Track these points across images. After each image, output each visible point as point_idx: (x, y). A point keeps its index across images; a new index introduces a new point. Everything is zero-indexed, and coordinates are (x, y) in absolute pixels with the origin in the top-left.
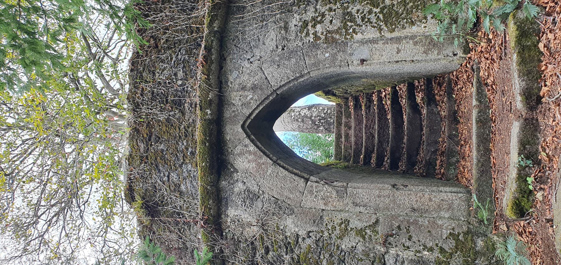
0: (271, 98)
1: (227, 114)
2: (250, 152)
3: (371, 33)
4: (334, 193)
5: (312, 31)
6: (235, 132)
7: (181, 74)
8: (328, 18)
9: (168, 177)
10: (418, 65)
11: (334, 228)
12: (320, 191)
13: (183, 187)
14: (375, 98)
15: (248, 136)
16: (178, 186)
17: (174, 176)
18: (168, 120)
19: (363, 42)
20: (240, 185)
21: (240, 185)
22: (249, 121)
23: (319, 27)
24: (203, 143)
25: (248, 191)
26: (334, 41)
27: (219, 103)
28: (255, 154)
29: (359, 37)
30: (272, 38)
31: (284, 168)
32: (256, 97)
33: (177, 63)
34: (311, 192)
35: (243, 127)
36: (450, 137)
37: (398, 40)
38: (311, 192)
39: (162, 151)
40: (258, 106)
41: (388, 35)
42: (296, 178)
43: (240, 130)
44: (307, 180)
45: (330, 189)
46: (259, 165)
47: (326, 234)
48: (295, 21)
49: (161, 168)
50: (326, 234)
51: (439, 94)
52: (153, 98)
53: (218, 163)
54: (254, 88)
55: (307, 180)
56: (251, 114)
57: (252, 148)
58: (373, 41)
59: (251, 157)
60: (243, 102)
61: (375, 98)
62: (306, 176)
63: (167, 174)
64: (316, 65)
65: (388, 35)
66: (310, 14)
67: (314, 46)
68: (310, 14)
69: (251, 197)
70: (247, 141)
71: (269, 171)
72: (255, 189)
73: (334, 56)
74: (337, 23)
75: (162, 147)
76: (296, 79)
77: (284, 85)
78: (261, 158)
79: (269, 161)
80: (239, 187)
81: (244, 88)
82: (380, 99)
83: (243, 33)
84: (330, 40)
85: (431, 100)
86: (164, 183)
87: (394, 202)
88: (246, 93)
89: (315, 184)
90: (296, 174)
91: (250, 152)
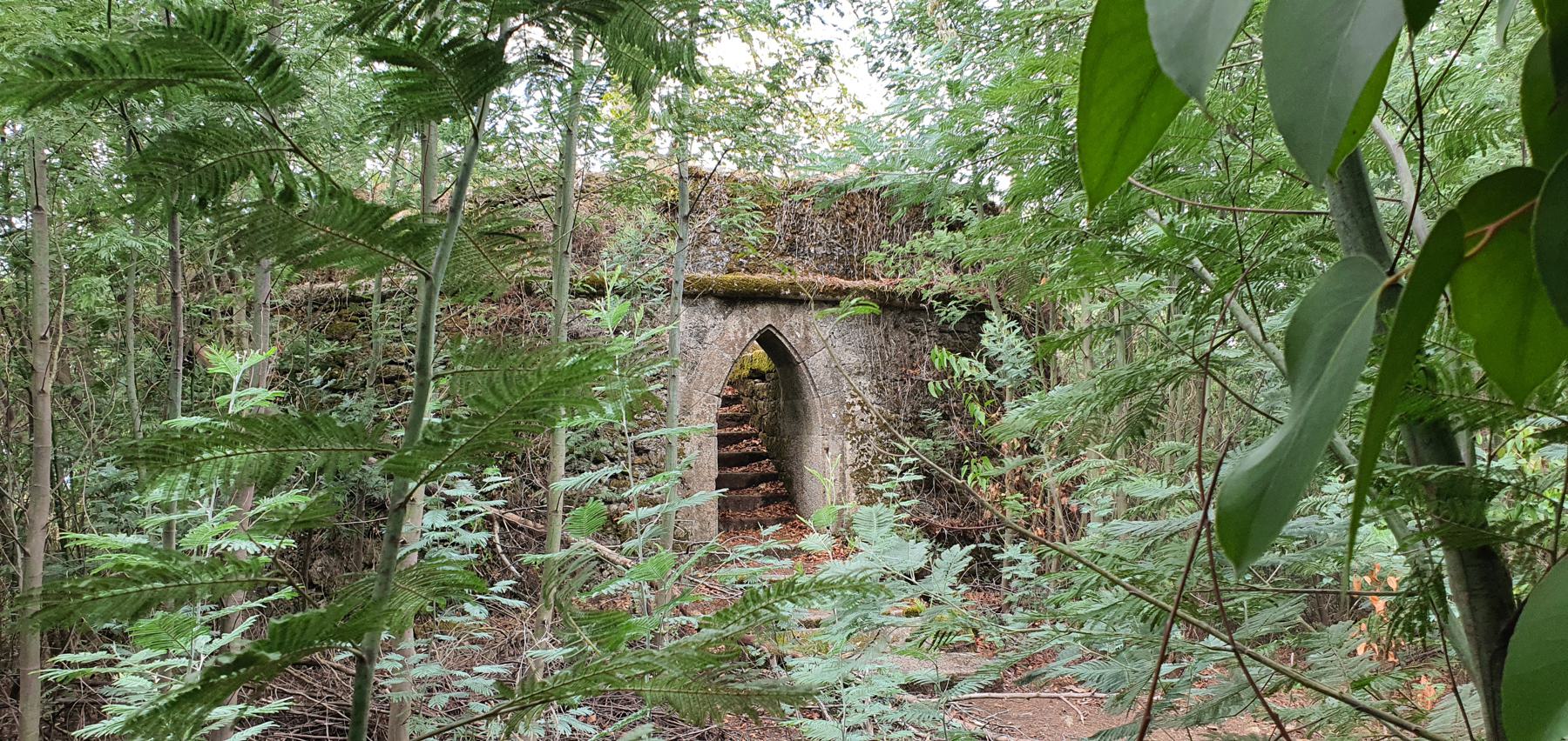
1: (782, 308)
3: (850, 457)
5: (855, 400)
6: (764, 316)
7: (821, 251)
8: (866, 417)
10: (819, 497)
13: (703, 250)
14: (746, 429)
16: (705, 243)
17: (715, 239)
19: (843, 449)
20: (711, 322)
21: (711, 322)
23: (858, 408)
26: (846, 423)
27: (795, 301)
28: (744, 339)
29: (848, 445)
30: (851, 358)
33: (831, 247)
34: (708, 401)
36: (742, 522)
37: (843, 480)
38: (708, 401)
41: (848, 472)
46: (732, 345)
48: (864, 381)
51: (777, 509)
52: (799, 217)
53: (733, 299)
54: (807, 339)
58: (843, 459)
60: (793, 327)
61: (746, 429)
64: (826, 405)
65: (848, 472)
66: (870, 399)
67: (843, 402)
68: (870, 399)
69: (700, 337)
70: (755, 331)
72: (709, 340)
73: (832, 422)
74: (861, 426)
81: (807, 328)
82: (748, 437)
83: (857, 326)
84: (847, 418)
85: (768, 500)
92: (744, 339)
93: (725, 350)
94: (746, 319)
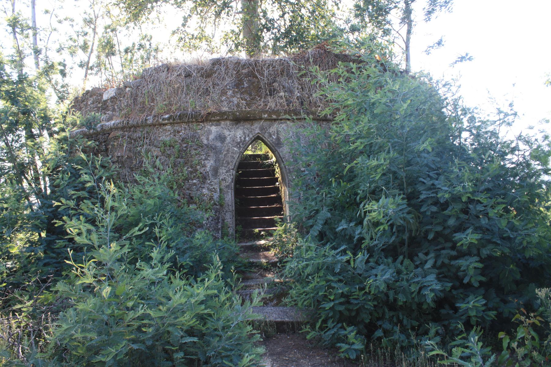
2: (245, 138)
4: (228, 184)
11: (212, 185)
22: (261, 136)
39: (243, 84)
42: (234, 164)
43: (257, 132)
44: (233, 169)
45: (229, 181)
46: (239, 143)
47: (209, 182)
50: (209, 182)
55: (233, 169)
59: (242, 138)
62: (235, 169)
70: (251, 136)
75: (246, 85)
76: (283, 162)
77: (280, 155)
78: (243, 144)
86: (226, 86)
87: (226, 212)
88: (276, 135)
89: (231, 174)
91: (245, 138)
92: (245, 141)
93: (235, 147)
94: (247, 132)
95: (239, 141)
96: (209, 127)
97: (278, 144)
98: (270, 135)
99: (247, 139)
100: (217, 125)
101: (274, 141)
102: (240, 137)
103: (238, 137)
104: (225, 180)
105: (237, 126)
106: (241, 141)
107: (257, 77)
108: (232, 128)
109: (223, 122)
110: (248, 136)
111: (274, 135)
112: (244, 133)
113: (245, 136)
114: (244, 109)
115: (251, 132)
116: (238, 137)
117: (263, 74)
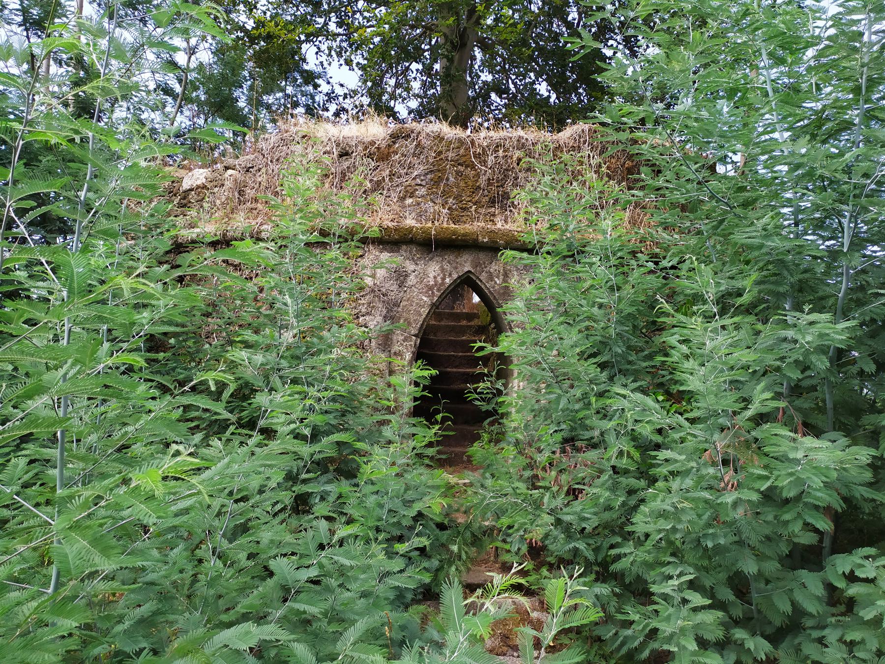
0: (495, 302)
1: (482, 256)
2: (443, 279)
6: (466, 264)
9: (421, 185)
12: (407, 349)
15: (459, 277)
17: (422, 191)
18: (479, 187)
22: (474, 278)
24: (454, 232)
25: (406, 276)
28: (443, 283)
31: (429, 313)
32: (497, 287)
35: (469, 272)
40: (488, 289)
43: (466, 269)
46: (431, 288)
49: (429, 177)
56: (481, 281)
57: (448, 280)
59: (439, 279)
63: (424, 183)
70: (455, 276)
71: (425, 299)
75: (452, 179)
78: (438, 290)
79: (436, 298)
80: (410, 266)
88: (501, 277)
89: (412, 343)
90: (422, 325)
91: (443, 279)
92: (443, 283)
94: (447, 267)
95: (432, 283)
96: (377, 253)
97: (504, 294)
98: (491, 277)
99: (448, 280)
100: (392, 251)
101: (497, 287)
102: (435, 277)
103: (431, 275)
104: (402, 356)
105: (430, 256)
106: (436, 285)
107: (473, 167)
108: (419, 258)
109: (404, 247)
110: (450, 275)
111: (498, 277)
112: (442, 270)
113: (444, 275)
114: (445, 225)
115: (456, 268)
116: (431, 275)
117: (485, 162)
